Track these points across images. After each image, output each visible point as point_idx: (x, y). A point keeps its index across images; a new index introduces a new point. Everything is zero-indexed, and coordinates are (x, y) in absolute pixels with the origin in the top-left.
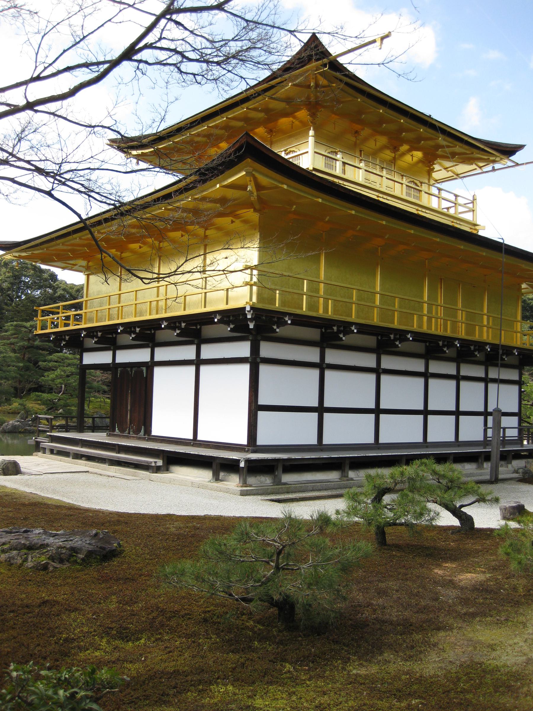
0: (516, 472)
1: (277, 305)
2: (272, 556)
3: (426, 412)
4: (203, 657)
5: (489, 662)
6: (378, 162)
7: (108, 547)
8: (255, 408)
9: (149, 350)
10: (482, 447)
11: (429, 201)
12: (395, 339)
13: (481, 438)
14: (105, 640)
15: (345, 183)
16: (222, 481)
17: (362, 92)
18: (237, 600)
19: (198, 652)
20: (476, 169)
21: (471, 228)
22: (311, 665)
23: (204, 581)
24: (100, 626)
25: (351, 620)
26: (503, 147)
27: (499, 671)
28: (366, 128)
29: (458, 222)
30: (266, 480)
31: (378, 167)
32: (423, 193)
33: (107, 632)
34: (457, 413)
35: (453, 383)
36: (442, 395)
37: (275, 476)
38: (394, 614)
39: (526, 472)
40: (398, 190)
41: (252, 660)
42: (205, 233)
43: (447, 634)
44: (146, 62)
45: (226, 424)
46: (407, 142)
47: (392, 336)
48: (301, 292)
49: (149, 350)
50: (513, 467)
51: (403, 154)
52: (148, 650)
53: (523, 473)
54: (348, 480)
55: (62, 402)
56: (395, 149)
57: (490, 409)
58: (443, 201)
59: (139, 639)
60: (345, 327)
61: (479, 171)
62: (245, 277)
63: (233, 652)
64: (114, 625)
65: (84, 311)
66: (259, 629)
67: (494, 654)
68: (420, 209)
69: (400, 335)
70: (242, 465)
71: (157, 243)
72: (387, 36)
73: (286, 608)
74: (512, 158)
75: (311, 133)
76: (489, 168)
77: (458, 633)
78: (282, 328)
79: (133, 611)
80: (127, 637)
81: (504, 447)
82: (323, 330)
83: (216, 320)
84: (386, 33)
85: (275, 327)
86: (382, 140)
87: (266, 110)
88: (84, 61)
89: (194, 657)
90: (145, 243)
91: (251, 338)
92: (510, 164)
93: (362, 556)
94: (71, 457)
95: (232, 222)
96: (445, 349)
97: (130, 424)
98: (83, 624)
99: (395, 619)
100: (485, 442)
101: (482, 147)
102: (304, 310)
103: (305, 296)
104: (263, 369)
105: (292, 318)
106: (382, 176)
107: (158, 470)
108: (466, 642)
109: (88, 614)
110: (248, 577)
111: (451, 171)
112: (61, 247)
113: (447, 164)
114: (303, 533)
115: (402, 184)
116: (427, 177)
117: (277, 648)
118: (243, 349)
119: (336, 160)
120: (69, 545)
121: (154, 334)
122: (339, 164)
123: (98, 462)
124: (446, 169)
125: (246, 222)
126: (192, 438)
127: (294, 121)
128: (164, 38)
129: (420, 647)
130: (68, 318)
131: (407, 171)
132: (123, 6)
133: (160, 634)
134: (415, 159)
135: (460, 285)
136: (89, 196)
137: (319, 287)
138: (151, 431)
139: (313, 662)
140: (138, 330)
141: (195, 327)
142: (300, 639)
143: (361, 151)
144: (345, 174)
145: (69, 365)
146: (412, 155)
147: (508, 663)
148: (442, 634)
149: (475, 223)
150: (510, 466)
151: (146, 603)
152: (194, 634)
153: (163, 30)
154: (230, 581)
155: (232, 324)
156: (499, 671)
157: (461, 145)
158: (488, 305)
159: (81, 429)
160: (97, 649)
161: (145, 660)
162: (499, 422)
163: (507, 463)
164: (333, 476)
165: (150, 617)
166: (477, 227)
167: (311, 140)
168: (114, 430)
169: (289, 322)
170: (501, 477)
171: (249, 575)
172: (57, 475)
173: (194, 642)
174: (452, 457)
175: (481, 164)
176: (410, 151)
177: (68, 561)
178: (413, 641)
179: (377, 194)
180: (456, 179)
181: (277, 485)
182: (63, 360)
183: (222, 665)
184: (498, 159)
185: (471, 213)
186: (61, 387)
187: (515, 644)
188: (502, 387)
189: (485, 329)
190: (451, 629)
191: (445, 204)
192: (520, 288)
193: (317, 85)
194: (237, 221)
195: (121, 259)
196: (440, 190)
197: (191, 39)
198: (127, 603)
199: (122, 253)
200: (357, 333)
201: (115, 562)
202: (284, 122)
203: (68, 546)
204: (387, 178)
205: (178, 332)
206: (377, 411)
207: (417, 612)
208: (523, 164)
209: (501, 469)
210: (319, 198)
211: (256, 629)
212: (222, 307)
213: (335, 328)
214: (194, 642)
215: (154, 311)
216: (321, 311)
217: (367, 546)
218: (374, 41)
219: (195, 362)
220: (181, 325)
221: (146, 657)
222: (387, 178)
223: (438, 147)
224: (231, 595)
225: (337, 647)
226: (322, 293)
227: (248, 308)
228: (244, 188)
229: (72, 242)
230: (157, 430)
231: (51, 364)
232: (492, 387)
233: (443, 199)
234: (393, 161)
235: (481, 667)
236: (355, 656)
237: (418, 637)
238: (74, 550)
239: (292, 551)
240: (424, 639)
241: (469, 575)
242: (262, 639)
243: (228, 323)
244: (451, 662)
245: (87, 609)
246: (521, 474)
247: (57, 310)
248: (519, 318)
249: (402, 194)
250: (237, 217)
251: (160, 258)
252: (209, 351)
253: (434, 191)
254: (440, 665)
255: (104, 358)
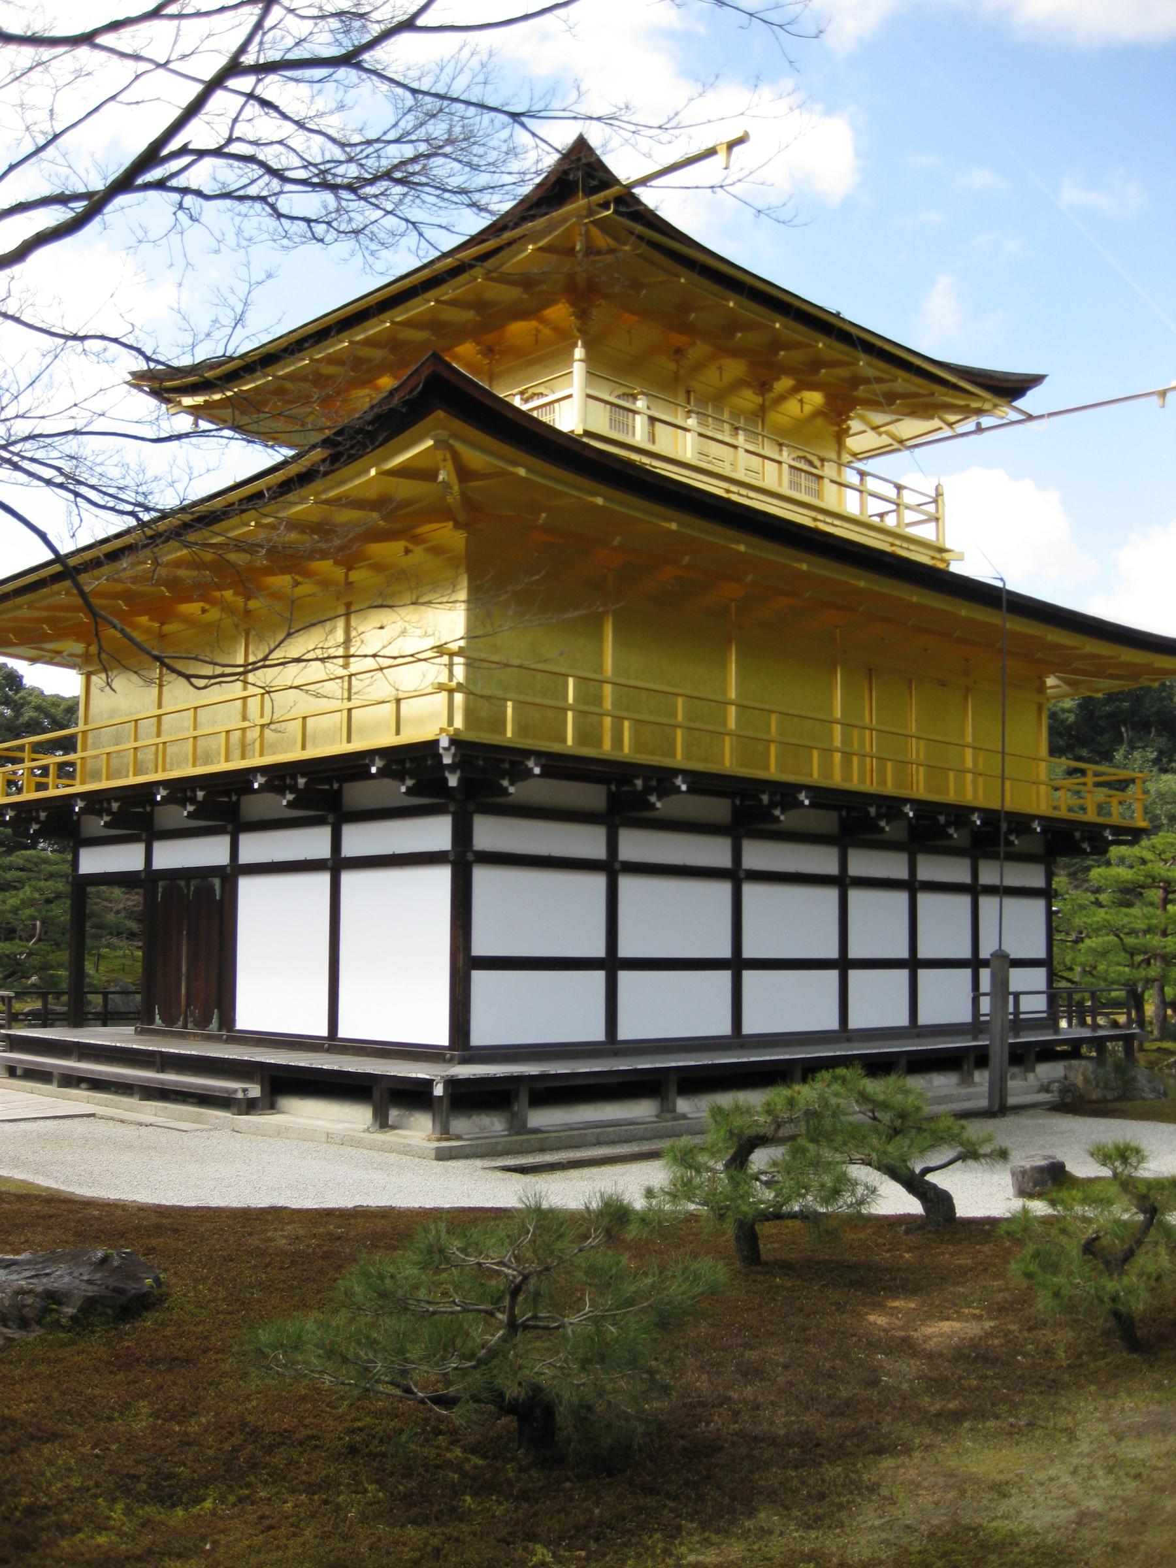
0: (1045, 1089)
1: (509, 734)
2: (500, 1299)
3: (843, 964)
4: (345, 1538)
5: (994, 1524)
6: (726, 416)
7: (132, 1287)
8: (465, 964)
9: (224, 841)
10: (970, 1037)
11: (841, 499)
12: (773, 804)
13: (966, 1017)
14: (119, 1506)
15: (656, 463)
16: (394, 1128)
17: (689, 264)
18: (422, 1401)
19: (336, 1526)
20: (940, 428)
21: (933, 558)
22: (593, 1546)
23: (345, 1360)
24: (110, 1472)
25: (682, 1437)
26: (998, 380)
27: (1017, 1545)
28: (698, 342)
29: (905, 545)
30: (493, 1125)
31: (726, 427)
32: (826, 481)
33: (125, 1486)
34: (913, 964)
35: (903, 897)
36: (878, 923)
37: (514, 1115)
38: (780, 1421)
39: (1067, 1088)
40: (772, 476)
41: (457, 1540)
42: (347, 575)
43: (899, 1461)
44: (198, 193)
45: (400, 1001)
46: (789, 371)
47: (765, 798)
48: (560, 704)
49: (224, 841)
50: (1037, 1078)
51: (782, 398)
52: (221, 1525)
53: (1060, 1091)
54: (675, 1119)
55: (36, 960)
56: (763, 387)
57: (984, 954)
58: (870, 498)
59: (199, 1500)
60: (662, 779)
61: (947, 432)
62: (436, 672)
63: (414, 1522)
64: (142, 1469)
65: (80, 754)
66: (476, 1467)
67: (1004, 1506)
68: (820, 517)
69: (783, 795)
70: (438, 1091)
71: (240, 601)
72: (740, 141)
73: (534, 1415)
74: (1018, 403)
75: (579, 352)
76: (970, 425)
77: (923, 1459)
78: (520, 784)
79: (186, 1434)
80: (171, 1496)
81: (1017, 1036)
82: (613, 788)
83: (374, 770)
84: (738, 134)
85: (505, 783)
86: (735, 368)
87: (479, 305)
88: (58, 191)
89: (325, 1537)
90: (213, 602)
91: (452, 809)
92: (1014, 416)
93: (702, 1293)
94: (55, 1083)
95: (407, 551)
96: (883, 824)
97: (188, 1005)
98: (70, 1470)
99: (782, 1432)
100: (976, 1026)
101: (953, 379)
102: (570, 742)
103: (570, 714)
104: (483, 878)
105: (543, 761)
106: (735, 447)
107: (250, 1106)
108: (941, 1481)
109: (83, 1445)
110: (445, 1349)
111: (886, 433)
112: (25, 613)
113: (878, 418)
114: (567, 1247)
115: (780, 463)
116: (835, 446)
117: (516, 1509)
118: (436, 833)
119: (634, 412)
120: (40, 1285)
121: (238, 802)
122: (640, 422)
123: (116, 1093)
124: (875, 428)
125: (437, 551)
126: (325, 1033)
127: (541, 327)
128: (239, 139)
129: (839, 1495)
130: (45, 770)
131: (791, 436)
132: (143, 66)
133: (249, 1485)
134: (808, 409)
135: (910, 681)
136: (77, 495)
137: (603, 692)
138: (233, 1021)
139: (597, 1540)
140: (200, 794)
141: (327, 787)
142: (568, 1485)
143: (688, 392)
144: (654, 442)
145: (51, 876)
146: (801, 401)
147: (1038, 1525)
148: (887, 1462)
149: (942, 546)
150: (1031, 1076)
151: (217, 1414)
152: (328, 1484)
153: (235, 121)
154: (406, 1360)
155: (411, 778)
156: (1017, 1545)
157: (906, 375)
158: (973, 727)
159: (78, 1019)
160: (102, 1528)
161: (213, 1549)
162: (1005, 982)
163: (1026, 1071)
164: (642, 1110)
165: (227, 1447)
166: (946, 556)
167: (578, 369)
168: (151, 1021)
169: (537, 771)
170: (1012, 1101)
171: (447, 1342)
172: (22, 1125)
173: (326, 1502)
174: (903, 1061)
175: (952, 418)
176: (796, 390)
177: (39, 1323)
178: (823, 1481)
179: (725, 485)
180: (897, 450)
181: (519, 1133)
182: (36, 865)
183: (389, 1553)
184: (987, 406)
185: (933, 524)
186: (35, 925)
187: (1051, 1479)
188: (1010, 903)
189: (969, 777)
190: (908, 1450)
191: (875, 506)
192: (1041, 688)
193: (590, 250)
194: (418, 552)
195: (162, 637)
196: (862, 474)
197: (299, 140)
198: (173, 1417)
199: (163, 624)
200: (690, 791)
201: (148, 1321)
202: (519, 330)
203: (40, 1289)
204: (747, 451)
205: (290, 797)
206: (737, 964)
207: (832, 1414)
208: (1042, 416)
209: (1011, 1084)
210: (596, 494)
211: (467, 1467)
212: (388, 739)
213: (639, 783)
214: (326, 1502)
215: (237, 753)
216: (607, 745)
217: (714, 1270)
218: (711, 152)
219: (330, 864)
220: (296, 782)
221: (215, 1543)
222: (747, 451)
223: (857, 381)
224: (408, 1390)
225: (651, 1502)
226: (608, 704)
227: (444, 742)
228: (429, 475)
229: (50, 600)
230: (247, 1018)
231: (10, 875)
232: (988, 904)
233: (871, 495)
234: (761, 413)
235: (976, 1536)
236: (692, 1521)
237: (833, 1471)
238: (53, 1297)
239: (544, 1287)
240: (847, 1476)
241: (946, 1326)
242: (483, 1487)
243: (400, 776)
244: (908, 1527)
245: (82, 1435)
246: (1056, 1094)
247: (18, 754)
248: (1043, 750)
249: (780, 485)
250: (417, 540)
251: (247, 632)
252: (360, 840)
253: (852, 477)
254: (884, 1535)
255: (125, 858)
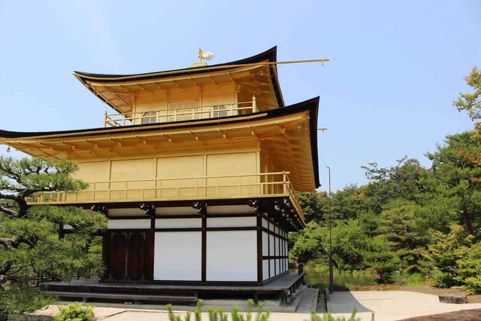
8: (260, 258)
9: (149, 221)
49: (149, 221)
72: (328, 60)
75: (254, 98)
138: (153, 277)
230: (158, 275)
